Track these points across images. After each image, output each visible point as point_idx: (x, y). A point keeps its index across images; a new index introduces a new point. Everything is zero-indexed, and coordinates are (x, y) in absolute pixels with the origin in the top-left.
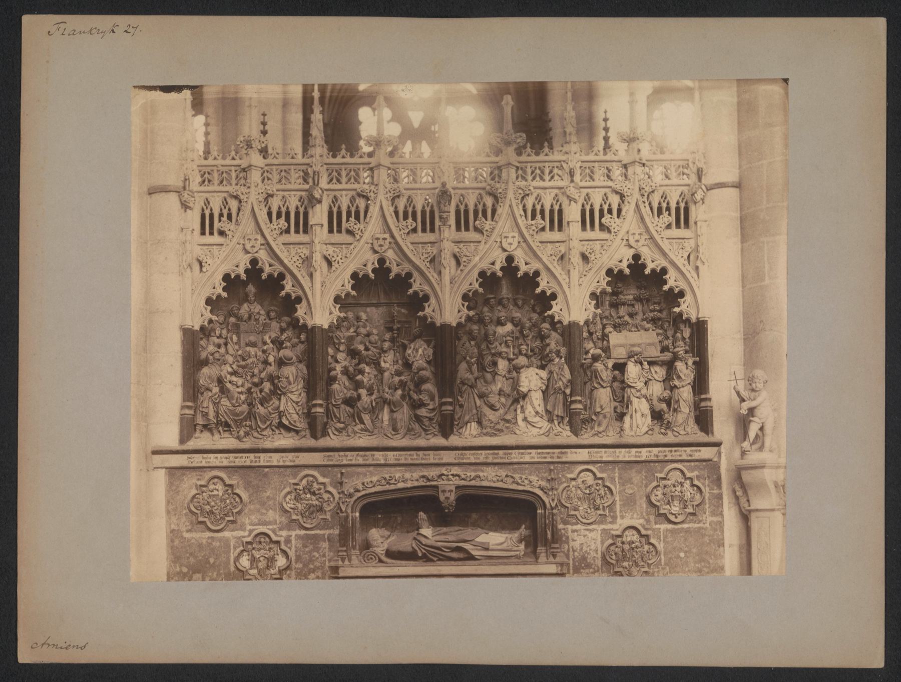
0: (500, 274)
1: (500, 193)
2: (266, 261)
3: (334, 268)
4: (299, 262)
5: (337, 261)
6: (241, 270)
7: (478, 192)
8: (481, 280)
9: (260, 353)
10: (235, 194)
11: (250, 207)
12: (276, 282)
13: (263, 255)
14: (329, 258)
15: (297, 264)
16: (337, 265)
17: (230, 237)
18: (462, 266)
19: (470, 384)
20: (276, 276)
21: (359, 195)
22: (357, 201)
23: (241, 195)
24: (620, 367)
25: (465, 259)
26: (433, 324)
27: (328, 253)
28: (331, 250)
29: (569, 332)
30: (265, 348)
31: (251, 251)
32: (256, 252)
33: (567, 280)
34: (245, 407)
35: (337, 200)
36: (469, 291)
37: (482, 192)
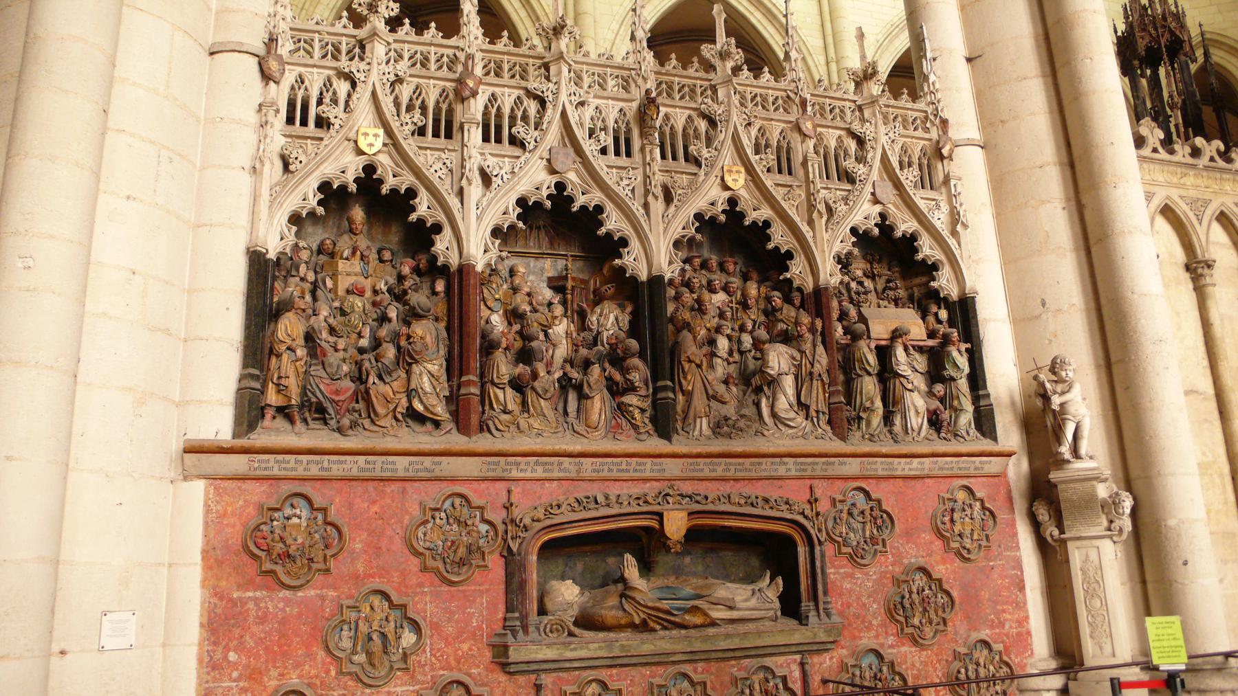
0: (723, 218)
1: (720, 115)
2: (389, 169)
3: (494, 185)
4: (443, 171)
5: (500, 176)
6: (350, 177)
7: (688, 112)
8: (697, 224)
9: (368, 306)
10: (347, 70)
11: (370, 88)
12: (403, 201)
13: (385, 162)
14: (488, 171)
15: (440, 173)
16: (500, 182)
17: (337, 126)
18: (675, 201)
19: (698, 362)
20: (403, 192)
21: (530, 94)
22: (525, 103)
23: (355, 72)
24: (884, 353)
25: (680, 191)
26: (634, 279)
27: (487, 163)
28: (491, 161)
29: (817, 301)
30: (378, 298)
31: (366, 150)
32: (374, 155)
33: (811, 234)
34: (348, 385)
35: (496, 100)
36: (684, 237)
37: (692, 112)
